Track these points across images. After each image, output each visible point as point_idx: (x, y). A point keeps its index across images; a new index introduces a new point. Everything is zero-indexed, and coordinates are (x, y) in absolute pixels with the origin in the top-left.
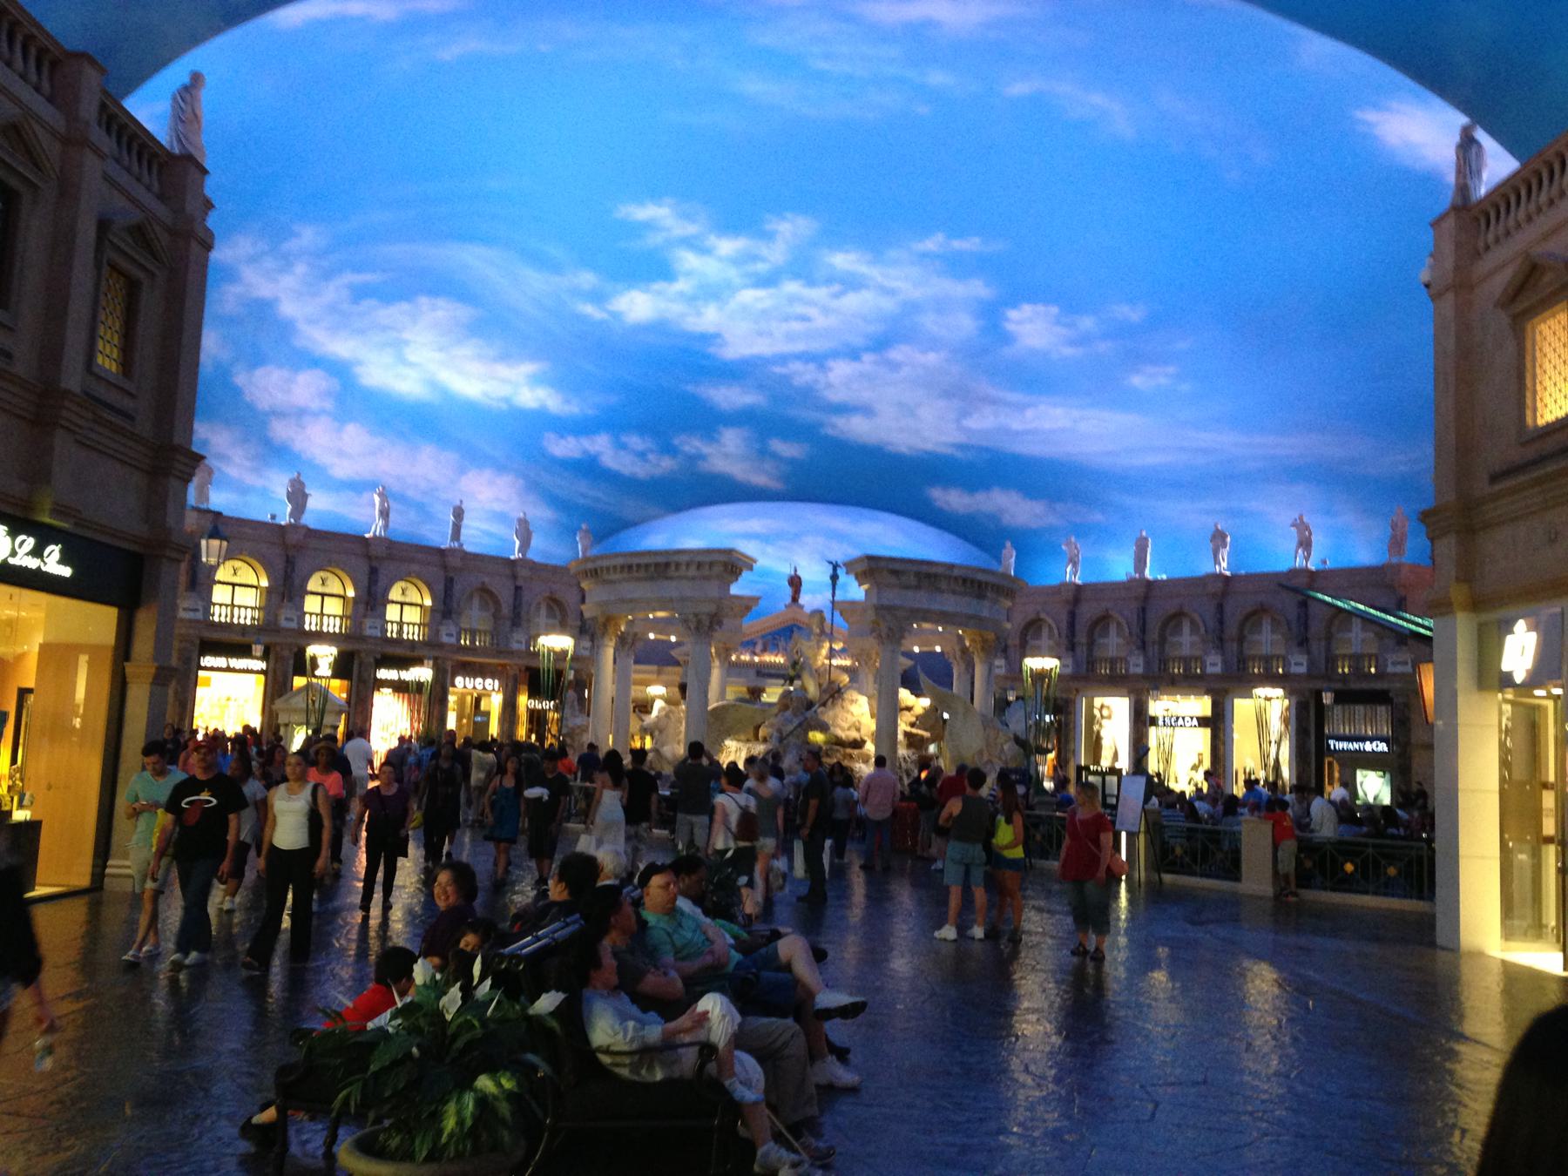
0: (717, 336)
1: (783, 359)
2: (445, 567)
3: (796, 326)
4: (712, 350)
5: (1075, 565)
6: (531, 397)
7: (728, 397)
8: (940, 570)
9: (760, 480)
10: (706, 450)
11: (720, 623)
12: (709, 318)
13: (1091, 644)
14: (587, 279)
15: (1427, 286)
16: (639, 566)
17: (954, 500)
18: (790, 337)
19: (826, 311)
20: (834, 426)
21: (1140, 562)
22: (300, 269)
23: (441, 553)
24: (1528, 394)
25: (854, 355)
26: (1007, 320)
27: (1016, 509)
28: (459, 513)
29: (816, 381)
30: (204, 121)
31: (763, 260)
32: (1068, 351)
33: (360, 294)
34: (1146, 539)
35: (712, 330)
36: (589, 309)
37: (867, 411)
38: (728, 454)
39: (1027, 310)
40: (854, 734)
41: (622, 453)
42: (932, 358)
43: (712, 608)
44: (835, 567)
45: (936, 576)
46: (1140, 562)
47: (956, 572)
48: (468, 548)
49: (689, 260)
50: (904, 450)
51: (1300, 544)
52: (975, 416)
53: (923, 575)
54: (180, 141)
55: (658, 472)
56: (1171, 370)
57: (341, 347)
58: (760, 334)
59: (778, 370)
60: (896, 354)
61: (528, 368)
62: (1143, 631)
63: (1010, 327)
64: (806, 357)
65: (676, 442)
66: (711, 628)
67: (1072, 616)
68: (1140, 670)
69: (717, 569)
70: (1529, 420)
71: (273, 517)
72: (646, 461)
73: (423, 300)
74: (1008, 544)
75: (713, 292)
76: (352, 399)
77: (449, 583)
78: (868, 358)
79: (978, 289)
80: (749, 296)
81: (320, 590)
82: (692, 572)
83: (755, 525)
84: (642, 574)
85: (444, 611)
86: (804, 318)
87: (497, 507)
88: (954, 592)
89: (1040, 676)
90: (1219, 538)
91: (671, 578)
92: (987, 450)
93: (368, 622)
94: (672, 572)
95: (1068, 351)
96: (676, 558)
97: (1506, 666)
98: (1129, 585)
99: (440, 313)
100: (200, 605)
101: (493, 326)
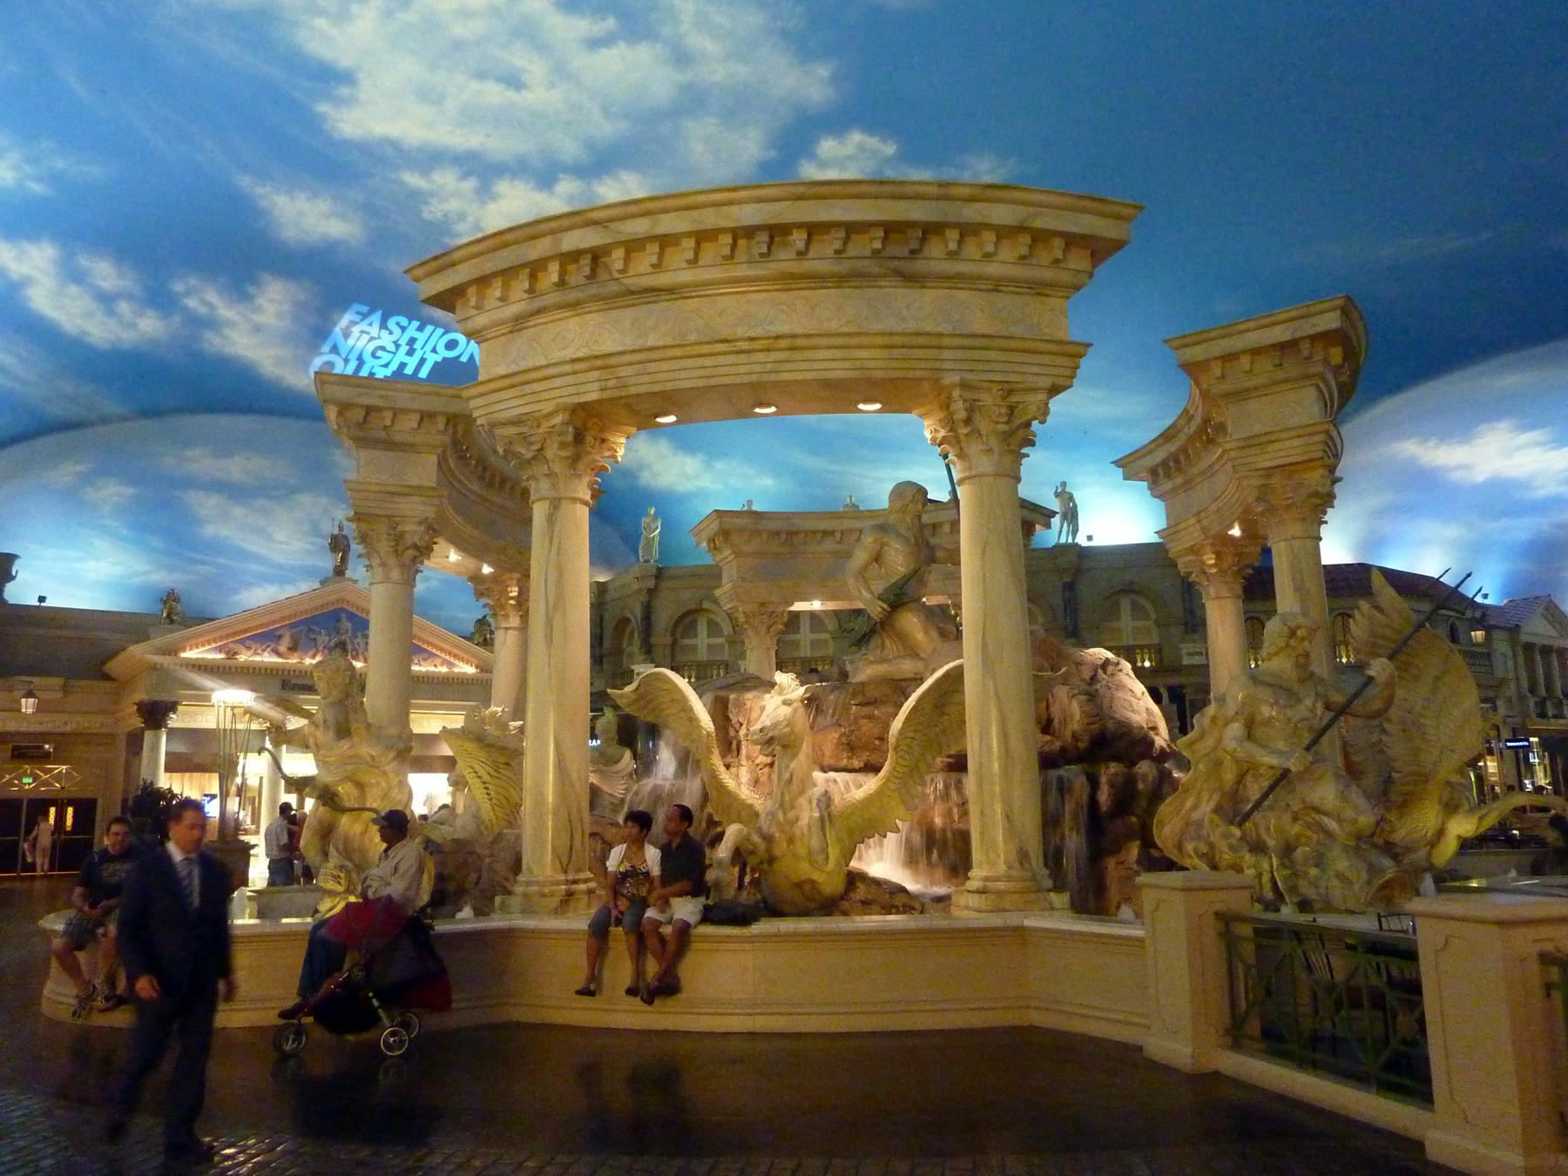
0: (347, 78)
1: (431, 159)
3: (494, 93)
10: (225, 312)
19: (560, 72)
35: (345, 62)
41: (73, 289)
55: (128, 337)
58: (428, 95)
59: (413, 179)
65: (178, 287)
72: (111, 313)
79: (813, 84)
86: (514, 81)
91: (911, 279)
94: (935, 257)
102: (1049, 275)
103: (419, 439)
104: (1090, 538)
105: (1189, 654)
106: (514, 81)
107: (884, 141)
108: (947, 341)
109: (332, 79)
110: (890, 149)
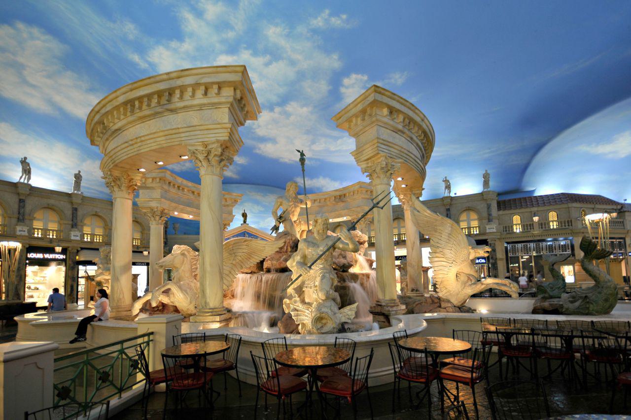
16: (140, 99)
20: (260, 149)
26: (343, 86)
37: (273, 140)
42: (305, 109)
50: (286, 160)
52: (317, 144)
55: (184, 168)
63: (343, 90)
78: (277, 109)
79: (333, 62)
82: (199, 99)
92: (319, 160)
94: (177, 103)
96: (179, 82)
99: (38, 43)
102: (216, 100)
103: (154, 185)
104: (455, 194)
105: (489, 229)
107: (363, 76)
108: (181, 130)
110: (365, 78)
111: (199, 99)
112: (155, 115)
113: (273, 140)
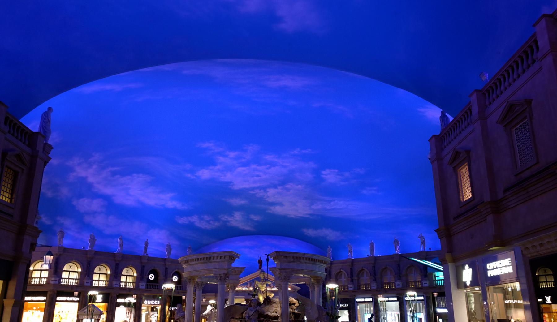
0: (231, 182)
1: (253, 189)
2: (142, 263)
3: (256, 178)
4: (230, 187)
5: (351, 252)
6: (171, 204)
7: (237, 202)
8: (300, 256)
9: (247, 228)
10: (230, 219)
11: (228, 277)
12: (228, 177)
13: (358, 280)
14: (188, 166)
15: (430, 159)
17: (310, 232)
18: (255, 182)
20: (270, 210)
21: (372, 250)
22: (95, 167)
23: (140, 257)
24: (461, 191)
25: (275, 187)
27: (331, 234)
28: (146, 244)
29: (264, 196)
30: (51, 123)
31: (244, 158)
32: (342, 183)
33: (114, 174)
34: (373, 243)
35: (229, 181)
36: (189, 175)
38: (237, 220)
39: (328, 171)
40: (275, 314)
42: (300, 186)
43: (225, 272)
44: (268, 256)
45: (300, 258)
46: (372, 250)
47: (306, 256)
48: (149, 255)
49: (221, 159)
50: (293, 216)
51: (422, 243)
53: (297, 258)
54: (43, 128)
56: (375, 188)
57: (108, 191)
59: (252, 192)
60: (288, 186)
61: (170, 195)
62: (375, 274)
63: (324, 176)
64: (260, 188)
66: (225, 279)
67: (351, 269)
68: (375, 288)
69: (227, 258)
70: (462, 200)
71: (84, 248)
72: (209, 224)
73: (135, 175)
74: (329, 247)
75: (229, 169)
76: (112, 207)
77: (143, 267)
79: (312, 165)
80: (240, 169)
81: (99, 272)
82: (219, 260)
83: (247, 243)
84: (202, 261)
85: (141, 277)
86: (258, 176)
87: (160, 241)
88: (306, 263)
89: (332, 291)
90: (396, 242)
91: (211, 262)
93: (114, 283)
94: (212, 260)
95: (342, 183)
97: (464, 280)
98: (367, 259)
100: (58, 279)
101: (158, 182)
106: (258, 176)
109: (228, 183)
111: (219, 260)
112: (205, 263)
113: (280, 204)
